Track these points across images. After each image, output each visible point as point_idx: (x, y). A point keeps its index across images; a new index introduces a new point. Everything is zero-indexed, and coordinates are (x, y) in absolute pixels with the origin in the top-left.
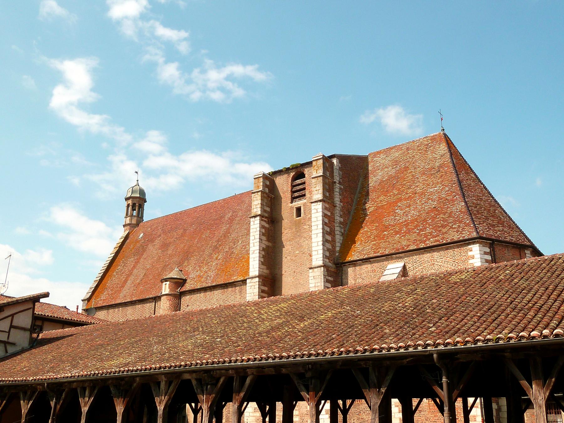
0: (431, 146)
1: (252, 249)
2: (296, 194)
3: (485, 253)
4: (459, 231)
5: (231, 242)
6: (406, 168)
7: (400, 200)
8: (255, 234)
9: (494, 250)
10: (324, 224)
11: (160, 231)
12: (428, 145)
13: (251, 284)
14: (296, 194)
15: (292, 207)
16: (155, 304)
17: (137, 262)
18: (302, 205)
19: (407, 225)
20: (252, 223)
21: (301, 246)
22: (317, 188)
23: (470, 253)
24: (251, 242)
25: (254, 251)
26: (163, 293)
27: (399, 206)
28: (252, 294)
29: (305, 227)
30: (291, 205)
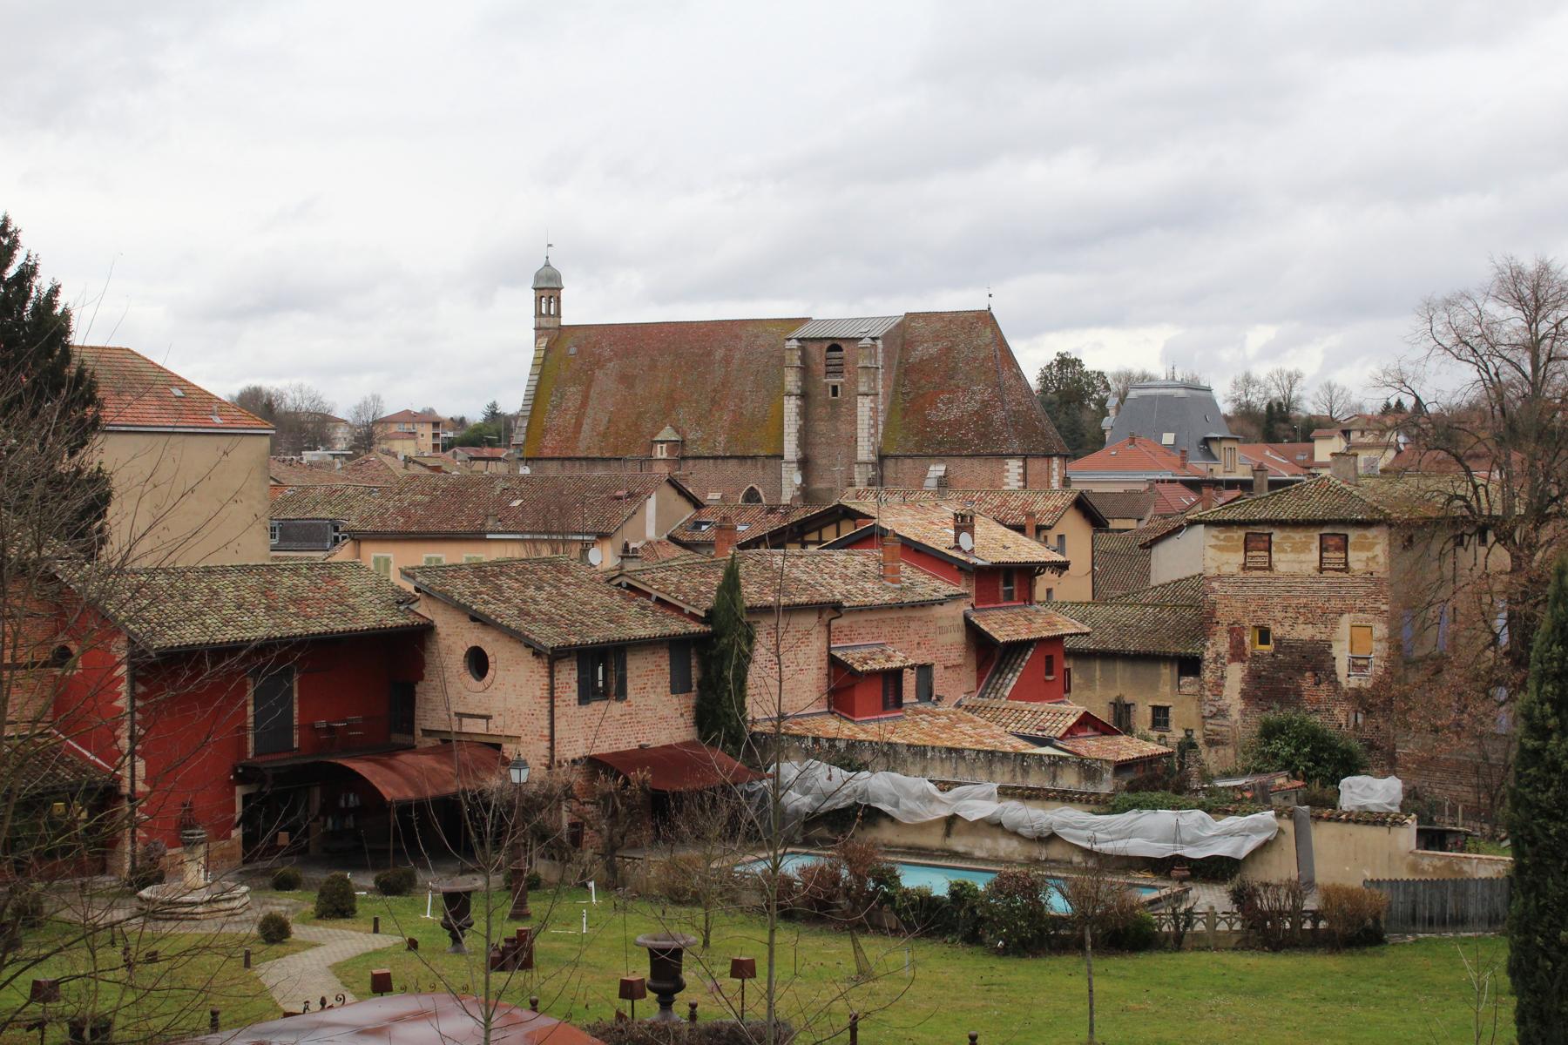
1: (786, 430)
3: (1019, 467)
6: (949, 349)
10: (871, 418)
11: (607, 353)
15: (827, 384)
20: (785, 402)
21: (837, 430)
26: (659, 456)
30: (825, 380)
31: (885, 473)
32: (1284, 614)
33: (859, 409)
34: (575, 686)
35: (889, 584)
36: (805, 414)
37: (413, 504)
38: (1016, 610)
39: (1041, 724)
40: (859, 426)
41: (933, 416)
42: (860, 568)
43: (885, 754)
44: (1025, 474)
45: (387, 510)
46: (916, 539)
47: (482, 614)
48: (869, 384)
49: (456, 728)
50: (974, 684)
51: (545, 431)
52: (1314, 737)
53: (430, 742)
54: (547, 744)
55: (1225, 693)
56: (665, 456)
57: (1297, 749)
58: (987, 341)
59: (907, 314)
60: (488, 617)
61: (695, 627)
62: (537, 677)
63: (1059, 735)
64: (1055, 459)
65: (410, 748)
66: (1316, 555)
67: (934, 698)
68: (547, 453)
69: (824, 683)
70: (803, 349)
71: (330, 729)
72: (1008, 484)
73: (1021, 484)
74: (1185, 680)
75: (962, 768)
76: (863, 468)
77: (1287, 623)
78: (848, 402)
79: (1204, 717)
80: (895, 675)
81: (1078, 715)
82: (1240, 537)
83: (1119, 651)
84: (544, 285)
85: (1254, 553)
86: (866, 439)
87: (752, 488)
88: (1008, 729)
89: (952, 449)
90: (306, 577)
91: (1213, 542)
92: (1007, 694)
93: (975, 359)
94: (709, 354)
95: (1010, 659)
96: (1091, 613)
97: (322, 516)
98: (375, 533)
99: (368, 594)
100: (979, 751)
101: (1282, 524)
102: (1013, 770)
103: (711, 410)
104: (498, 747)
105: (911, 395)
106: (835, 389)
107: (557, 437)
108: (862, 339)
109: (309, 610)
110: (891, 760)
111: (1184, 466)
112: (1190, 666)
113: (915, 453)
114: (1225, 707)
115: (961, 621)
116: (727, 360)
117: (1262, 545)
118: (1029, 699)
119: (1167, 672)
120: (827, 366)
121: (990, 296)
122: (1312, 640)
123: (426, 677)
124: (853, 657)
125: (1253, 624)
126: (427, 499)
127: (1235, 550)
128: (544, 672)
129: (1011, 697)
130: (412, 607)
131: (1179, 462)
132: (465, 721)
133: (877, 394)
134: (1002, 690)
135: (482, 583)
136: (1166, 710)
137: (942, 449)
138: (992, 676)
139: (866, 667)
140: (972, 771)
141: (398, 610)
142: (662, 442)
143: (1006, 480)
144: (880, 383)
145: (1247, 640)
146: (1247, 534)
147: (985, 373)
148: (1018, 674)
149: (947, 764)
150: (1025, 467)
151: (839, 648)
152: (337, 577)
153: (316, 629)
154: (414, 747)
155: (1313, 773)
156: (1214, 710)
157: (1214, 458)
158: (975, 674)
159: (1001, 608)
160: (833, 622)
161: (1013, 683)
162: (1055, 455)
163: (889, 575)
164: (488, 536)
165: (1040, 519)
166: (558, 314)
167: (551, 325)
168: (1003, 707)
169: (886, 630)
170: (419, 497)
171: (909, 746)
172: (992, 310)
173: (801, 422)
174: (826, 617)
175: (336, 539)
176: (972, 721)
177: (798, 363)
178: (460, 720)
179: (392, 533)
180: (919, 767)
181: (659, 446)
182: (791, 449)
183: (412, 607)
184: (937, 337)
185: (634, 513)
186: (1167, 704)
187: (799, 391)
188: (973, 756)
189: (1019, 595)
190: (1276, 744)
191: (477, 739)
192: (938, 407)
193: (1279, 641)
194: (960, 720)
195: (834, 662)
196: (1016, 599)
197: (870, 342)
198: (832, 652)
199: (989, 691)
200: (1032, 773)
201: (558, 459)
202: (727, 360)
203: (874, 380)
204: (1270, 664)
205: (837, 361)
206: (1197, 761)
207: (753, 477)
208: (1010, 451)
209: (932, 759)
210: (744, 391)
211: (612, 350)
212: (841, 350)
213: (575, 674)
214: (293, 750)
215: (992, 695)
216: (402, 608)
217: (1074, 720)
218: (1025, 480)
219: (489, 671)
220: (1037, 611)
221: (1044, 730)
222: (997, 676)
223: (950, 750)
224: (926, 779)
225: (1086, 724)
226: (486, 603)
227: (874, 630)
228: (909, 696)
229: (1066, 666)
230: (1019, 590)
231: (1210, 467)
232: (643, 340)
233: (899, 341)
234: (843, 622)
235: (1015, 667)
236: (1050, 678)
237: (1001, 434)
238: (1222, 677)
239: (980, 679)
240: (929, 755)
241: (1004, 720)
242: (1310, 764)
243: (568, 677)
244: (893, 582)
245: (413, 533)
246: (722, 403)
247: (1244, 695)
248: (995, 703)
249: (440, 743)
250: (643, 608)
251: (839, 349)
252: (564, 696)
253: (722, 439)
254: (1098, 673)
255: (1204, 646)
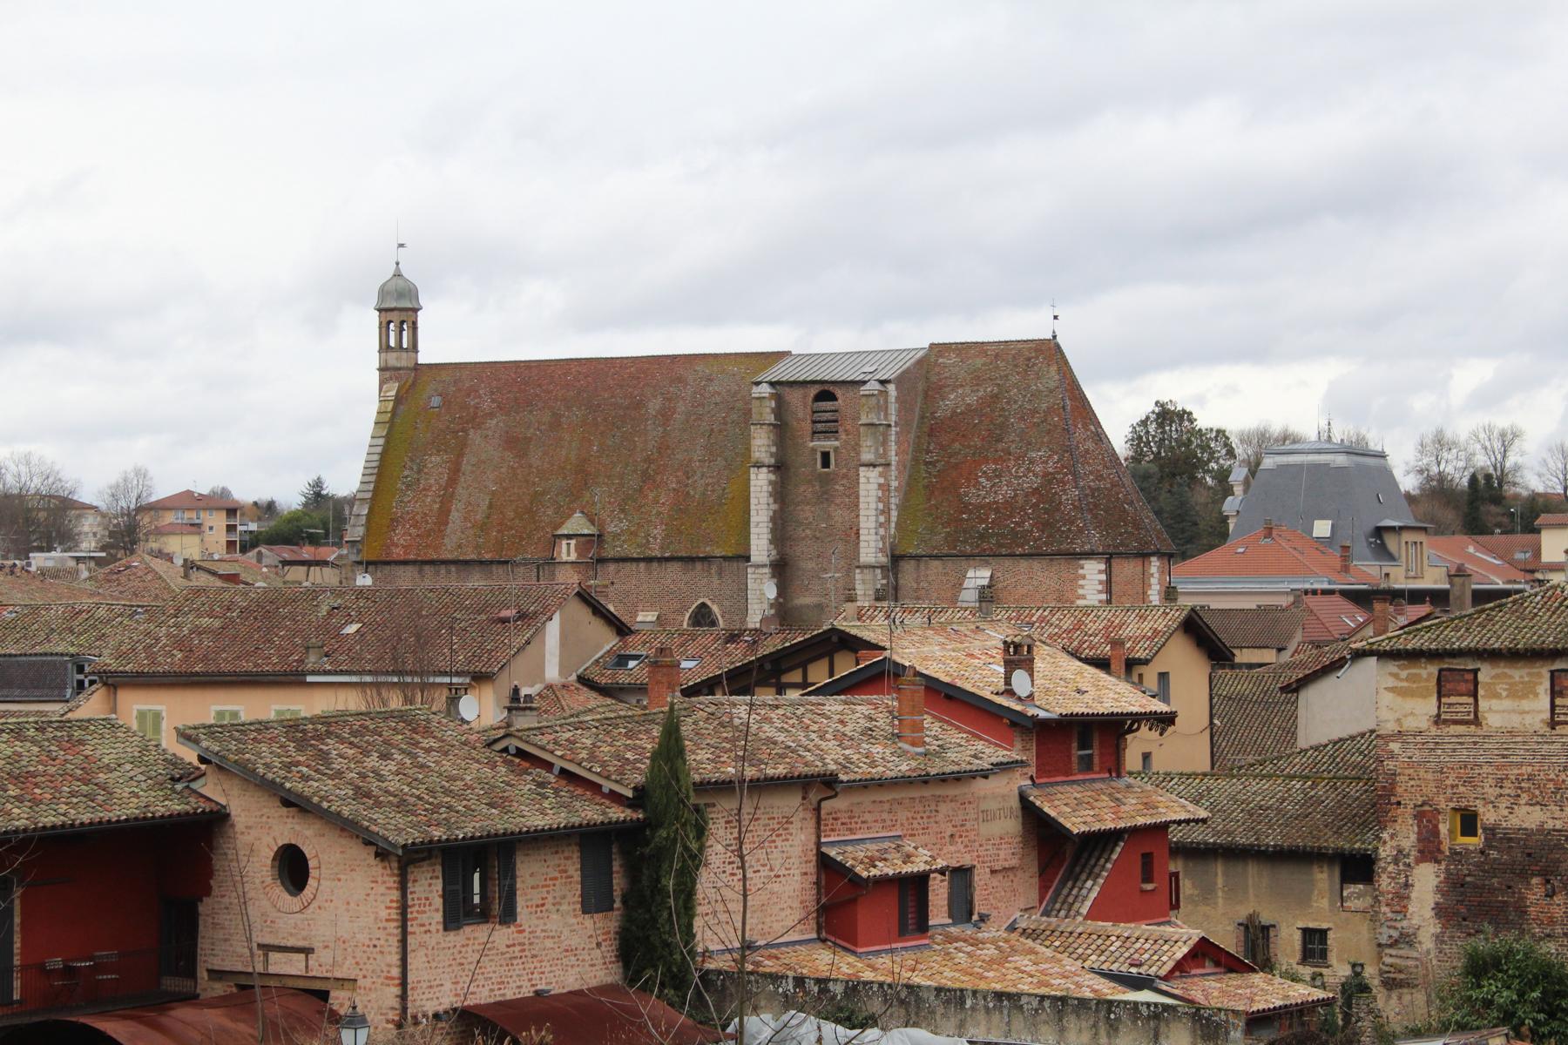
0: (1034, 364)
1: (753, 519)
2: (819, 426)
3: (1100, 572)
4: (1067, 537)
5: (678, 470)
6: (995, 397)
7: (986, 460)
8: (759, 495)
9: (1110, 566)
10: (880, 499)
11: (487, 405)
12: (1029, 359)
13: (754, 576)
14: (819, 426)
15: (814, 450)
16: (538, 573)
17: (455, 472)
18: (832, 451)
19: (997, 511)
20: (753, 477)
21: (830, 517)
22: (869, 444)
23: (1081, 572)
24: (752, 507)
25: (758, 523)
26: (565, 558)
27: (985, 472)
28: (758, 592)
29: (837, 487)
30: (811, 444)
31: (901, 582)
32: (1498, 791)
33: (862, 487)
34: (438, 902)
35: (906, 747)
36: (781, 493)
37: (198, 631)
38: (1098, 785)
39: (1136, 956)
40: (862, 513)
41: (973, 496)
42: (864, 723)
43: (902, 1002)
44: (1109, 582)
45: (158, 640)
46: (947, 679)
47: (300, 796)
48: (877, 450)
49: (260, 968)
50: (1034, 895)
51: (394, 522)
52: (1546, 976)
53: (220, 989)
54: (397, 991)
55: (1411, 909)
56: (573, 557)
57: (1521, 994)
58: (1052, 384)
59: (932, 346)
60: (308, 800)
61: (618, 813)
62: (382, 889)
63: (1163, 972)
64: (1153, 559)
65: (191, 998)
66: (1544, 702)
67: (975, 917)
68: (398, 553)
69: (810, 895)
70: (778, 398)
71: (69, 971)
72: (1083, 597)
73: (1104, 597)
74: (1351, 889)
75: (1018, 1022)
76: (868, 575)
77: (1504, 804)
78: (845, 476)
79: (1379, 945)
80: (919, 883)
81: (1191, 943)
82: (1430, 674)
83: (1252, 845)
84: (393, 305)
85: (1453, 699)
86: (873, 531)
87: (703, 605)
88: (1087, 965)
89: (1001, 546)
90: (34, 742)
91: (1391, 682)
92: (1084, 911)
93: (1035, 411)
94: (639, 405)
95: (1088, 860)
96: (1209, 790)
97: (59, 649)
98: (139, 674)
99: (128, 767)
100: (1043, 998)
101: (1493, 656)
102: (1095, 1026)
103: (641, 490)
104: (324, 996)
105: (939, 466)
106: (826, 457)
107: (413, 531)
108: (864, 383)
109: (37, 791)
110: (912, 1009)
111: (1346, 569)
112: (1358, 868)
113: (945, 550)
114: (1411, 931)
115: (1015, 803)
116: (665, 415)
117: (1463, 687)
118: (1117, 920)
119: (1323, 879)
120: (814, 422)
121: (1056, 317)
122: (1541, 829)
123: (216, 891)
124: (854, 857)
125: (1452, 805)
126: (217, 623)
127: (1424, 695)
128: (392, 881)
129: (1092, 915)
130: (194, 785)
131: (1338, 564)
132: (274, 956)
133: (889, 465)
134: (1077, 905)
135: (299, 749)
136: (1322, 934)
137: (985, 546)
138: (1063, 883)
139: (874, 872)
140: (1033, 1027)
141: (173, 790)
142: (569, 537)
143: (1081, 592)
144: (893, 447)
145: (1444, 829)
146: (1440, 671)
147: (1049, 432)
148: (1101, 881)
149: (996, 1017)
150: (1109, 572)
151: (832, 844)
152: (81, 742)
153: (48, 819)
154: (196, 997)
155: (1545, 1030)
156: (1395, 934)
157: (1391, 557)
158: (1036, 880)
159: (1074, 782)
160: (824, 804)
161: (1093, 895)
162: (1153, 554)
163: (907, 733)
164: (310, 679)
165: (1132, 649)
166: (414, 346)
167: (403, 363)
168: (1080, 930)
169: (903, 815)
170: (205, 621)
171: (939, 990)
172: (1059, 339)
173: (774, 507)
174: (814, 797)
175: (81, 684)
176: (1032, 951)
177: (771, 418)
178: (266, 956)
179: (165, 674)
180: (953, 1021)
181: (564, 542)
182: (760, 546)
183: (194, 785)
184: (977, 380)
185: (528, 643)
186: (1324, 926)
187: (772, 461)
188: (1035, 1003)
189: (1102, 762)
190: (1490, 987)
191: (290, 983)
192: (980, 483)
193: (1491, 831)
194: (1014, 950)
195: (826, 865)
196: (1096, 768)
197: (878, 386)
198: (824, 849)
199: (1058, 906)
200: (1123, 1029)
201: (414, 562)
202: (665, 415)
203: (885, 443)
204: (1478, 865)
205: (828, 416)
206: (1370, 1012)
207: (706, 589)
208: (1087, 547)
209: (973, 1008)
210: (690, 460)
211: (493, 401)
212: (836, 399)
213: (438, 885)
214: (12, 1002)
215: (1063, 913)
216: (179, 787)
217: (1185, 950)
218: (1109, 591)
219: (311, 881)
220: (1129, 786)
221: (1140, 965)
222: (1070, 884)
223: (999, 996)
224: (964, 1040)
225: (1204, 955)
226: (305, 778)
227: (885, 816)
228: (938, 913)
229: (1172, 868)
230: (1101, 755)
231: (1385, 570)
232: (539, 385)
233: (921, 386)
234: (839, 804)
235: (1096, 870)
236: (1149, 887)
237: (1072, 523)
238: (1407, 885)
239: (1043, 889)
240: (969, 1003)
241: (1080, 951)
242: (1541, 1016)
243: (428, 889)
244: (913, 744)
245: (197, 674)
246: (658, 478)
247: (1440, 911)
248: (1067, 925)
249: (234, 990)
250: (541, 785)
251: (832, 397)
252: (423, 918)
253: (658, 532)
254: (1220, 881)
255: (1378, 838)
